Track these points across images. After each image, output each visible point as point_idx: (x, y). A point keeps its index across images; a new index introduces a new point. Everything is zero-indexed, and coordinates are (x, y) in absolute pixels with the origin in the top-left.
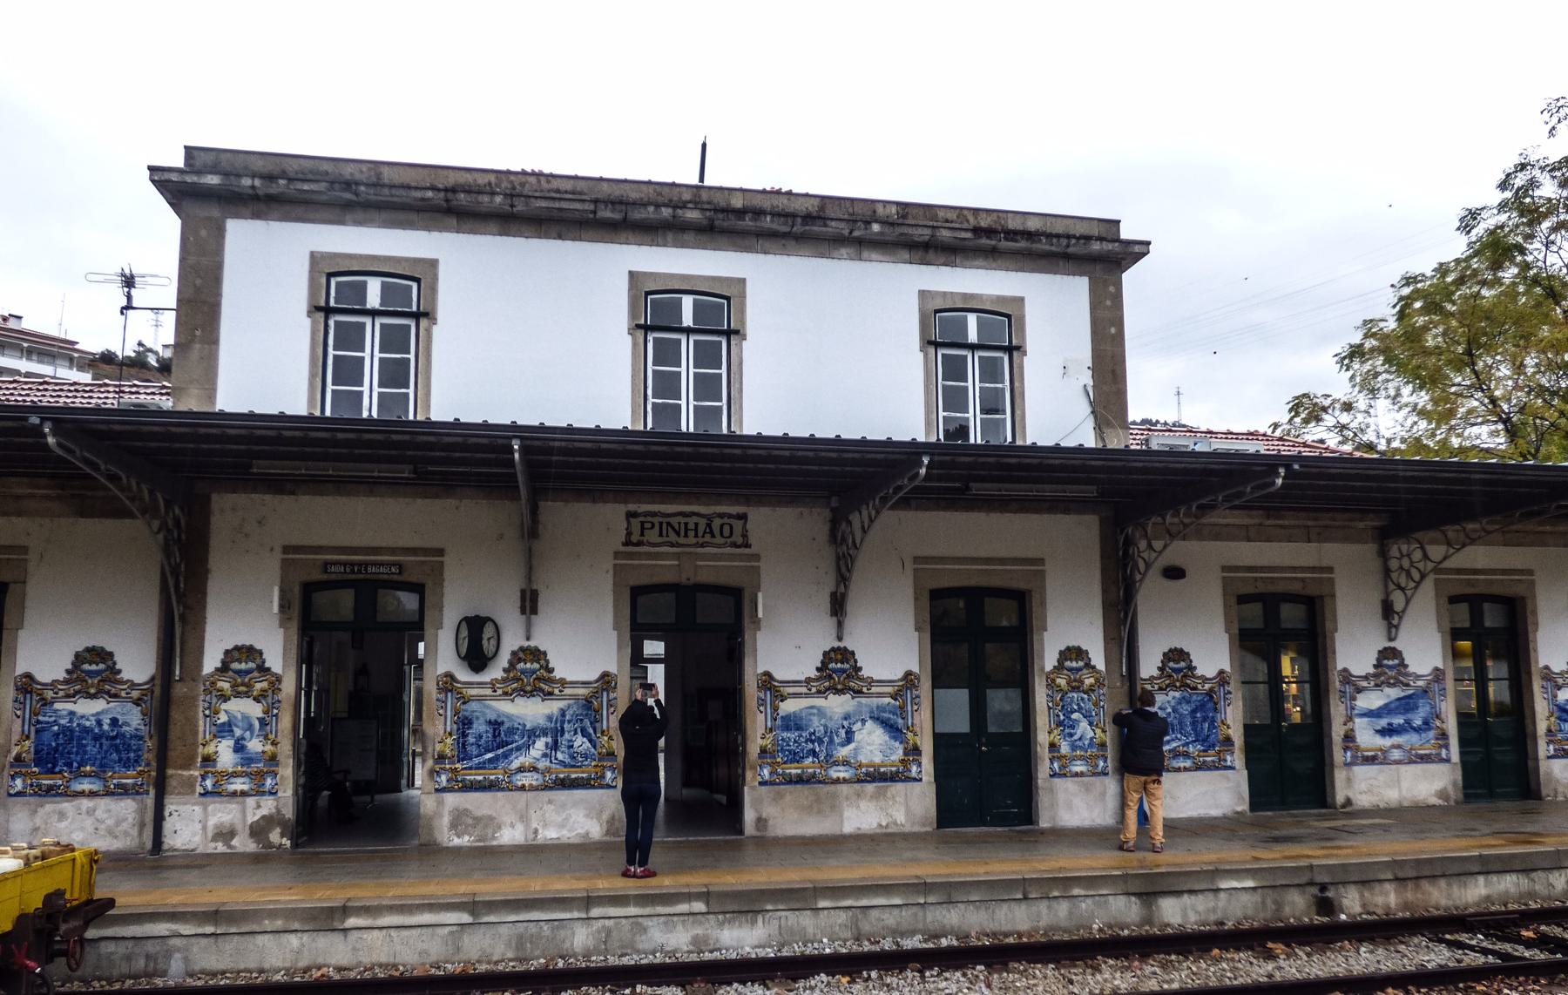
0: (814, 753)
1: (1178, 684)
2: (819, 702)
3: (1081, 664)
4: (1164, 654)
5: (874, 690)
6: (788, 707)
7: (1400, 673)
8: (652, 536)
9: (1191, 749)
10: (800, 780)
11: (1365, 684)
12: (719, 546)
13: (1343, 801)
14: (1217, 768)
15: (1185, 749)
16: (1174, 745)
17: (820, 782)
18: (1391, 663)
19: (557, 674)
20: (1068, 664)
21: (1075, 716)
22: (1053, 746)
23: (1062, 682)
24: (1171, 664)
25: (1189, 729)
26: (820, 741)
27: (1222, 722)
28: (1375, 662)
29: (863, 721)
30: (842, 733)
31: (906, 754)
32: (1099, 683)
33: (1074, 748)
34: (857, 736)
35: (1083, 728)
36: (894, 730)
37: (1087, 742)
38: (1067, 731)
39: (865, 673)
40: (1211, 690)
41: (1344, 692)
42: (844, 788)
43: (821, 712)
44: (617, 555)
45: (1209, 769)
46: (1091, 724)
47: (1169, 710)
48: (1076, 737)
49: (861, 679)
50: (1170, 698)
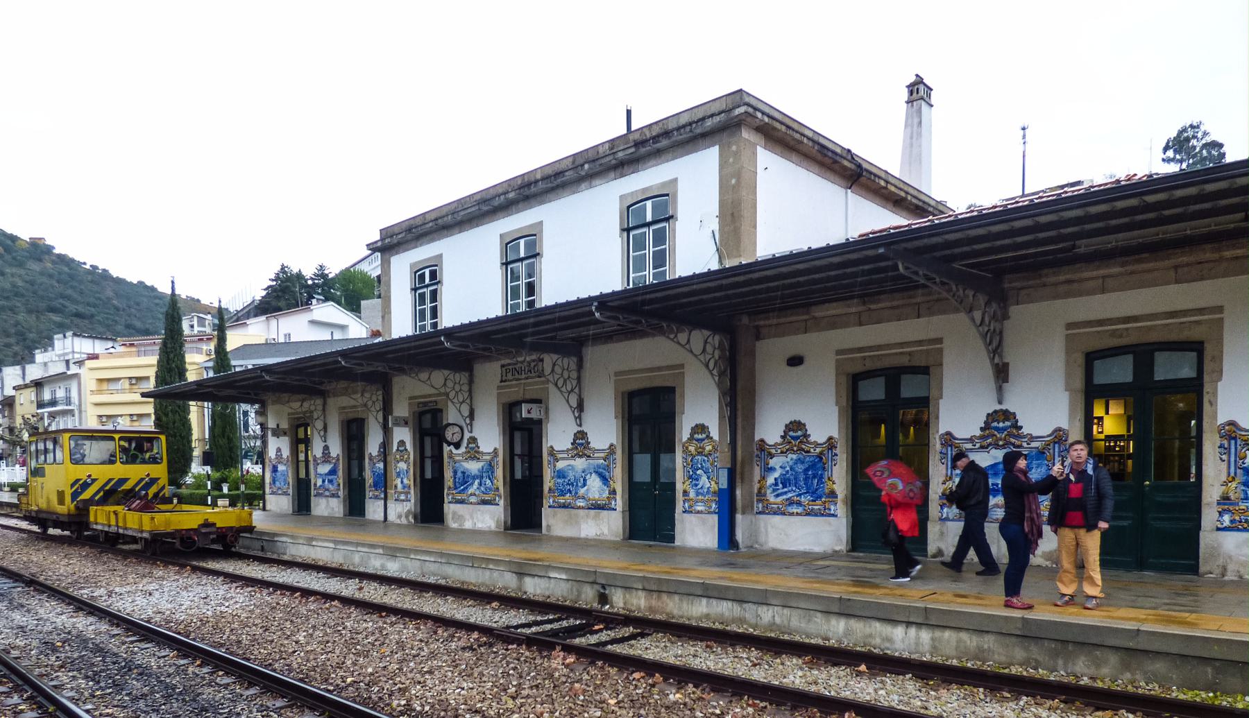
0: (570, 491)
1: (795, 449)
2: (572, 462)
3: (704, 436)
4: (786, 426)
5: (596, 455)
6: (561, 465)
7: (1010, 435)
8: (510, 376)
9: (803, 499)
10: (564, 506)
11: (969, 446)
12: (532, 378)
13: (934, 551)
14: (822, 515)
15: (798, 498)
16: (790, 495)
17: (573, 508)
18: (1001, 425)
19: (481, 450)
20: (696, 436)
21: (699, 472)
22: (685, 493)
23: (692, 449)
24: (791, 433)
25: (802, 483)
26: (573, 485)
27: (829, 479)
28: (983, 425)
29: (591, 474)
30: (582, 479)
31: (609, 494)
32: (715, 449)
33: (698, 494)
34: (588, 483)
35: (704, 480)
36: (605, 480)
37: (705, 490)
38: (694, 482)
39: (592, 445)
40: (821, 453)
41: (947, 454)
42: (581, 512)
43: (573, 468)
44: (499, 388)
45: (816, 515)
46: (708, 478)
47: (788, 468)
48: (699, 487)
49: (589, 449)
50: (789, 459)
